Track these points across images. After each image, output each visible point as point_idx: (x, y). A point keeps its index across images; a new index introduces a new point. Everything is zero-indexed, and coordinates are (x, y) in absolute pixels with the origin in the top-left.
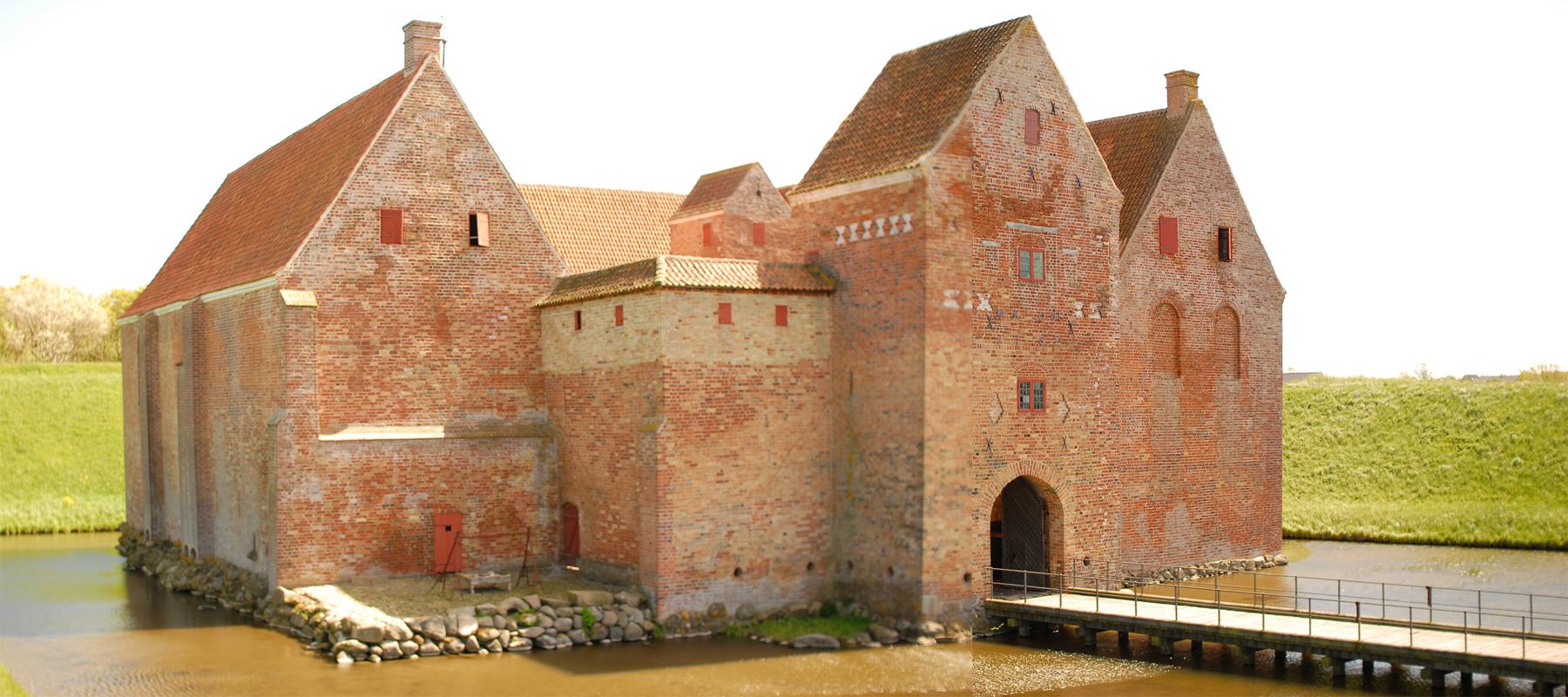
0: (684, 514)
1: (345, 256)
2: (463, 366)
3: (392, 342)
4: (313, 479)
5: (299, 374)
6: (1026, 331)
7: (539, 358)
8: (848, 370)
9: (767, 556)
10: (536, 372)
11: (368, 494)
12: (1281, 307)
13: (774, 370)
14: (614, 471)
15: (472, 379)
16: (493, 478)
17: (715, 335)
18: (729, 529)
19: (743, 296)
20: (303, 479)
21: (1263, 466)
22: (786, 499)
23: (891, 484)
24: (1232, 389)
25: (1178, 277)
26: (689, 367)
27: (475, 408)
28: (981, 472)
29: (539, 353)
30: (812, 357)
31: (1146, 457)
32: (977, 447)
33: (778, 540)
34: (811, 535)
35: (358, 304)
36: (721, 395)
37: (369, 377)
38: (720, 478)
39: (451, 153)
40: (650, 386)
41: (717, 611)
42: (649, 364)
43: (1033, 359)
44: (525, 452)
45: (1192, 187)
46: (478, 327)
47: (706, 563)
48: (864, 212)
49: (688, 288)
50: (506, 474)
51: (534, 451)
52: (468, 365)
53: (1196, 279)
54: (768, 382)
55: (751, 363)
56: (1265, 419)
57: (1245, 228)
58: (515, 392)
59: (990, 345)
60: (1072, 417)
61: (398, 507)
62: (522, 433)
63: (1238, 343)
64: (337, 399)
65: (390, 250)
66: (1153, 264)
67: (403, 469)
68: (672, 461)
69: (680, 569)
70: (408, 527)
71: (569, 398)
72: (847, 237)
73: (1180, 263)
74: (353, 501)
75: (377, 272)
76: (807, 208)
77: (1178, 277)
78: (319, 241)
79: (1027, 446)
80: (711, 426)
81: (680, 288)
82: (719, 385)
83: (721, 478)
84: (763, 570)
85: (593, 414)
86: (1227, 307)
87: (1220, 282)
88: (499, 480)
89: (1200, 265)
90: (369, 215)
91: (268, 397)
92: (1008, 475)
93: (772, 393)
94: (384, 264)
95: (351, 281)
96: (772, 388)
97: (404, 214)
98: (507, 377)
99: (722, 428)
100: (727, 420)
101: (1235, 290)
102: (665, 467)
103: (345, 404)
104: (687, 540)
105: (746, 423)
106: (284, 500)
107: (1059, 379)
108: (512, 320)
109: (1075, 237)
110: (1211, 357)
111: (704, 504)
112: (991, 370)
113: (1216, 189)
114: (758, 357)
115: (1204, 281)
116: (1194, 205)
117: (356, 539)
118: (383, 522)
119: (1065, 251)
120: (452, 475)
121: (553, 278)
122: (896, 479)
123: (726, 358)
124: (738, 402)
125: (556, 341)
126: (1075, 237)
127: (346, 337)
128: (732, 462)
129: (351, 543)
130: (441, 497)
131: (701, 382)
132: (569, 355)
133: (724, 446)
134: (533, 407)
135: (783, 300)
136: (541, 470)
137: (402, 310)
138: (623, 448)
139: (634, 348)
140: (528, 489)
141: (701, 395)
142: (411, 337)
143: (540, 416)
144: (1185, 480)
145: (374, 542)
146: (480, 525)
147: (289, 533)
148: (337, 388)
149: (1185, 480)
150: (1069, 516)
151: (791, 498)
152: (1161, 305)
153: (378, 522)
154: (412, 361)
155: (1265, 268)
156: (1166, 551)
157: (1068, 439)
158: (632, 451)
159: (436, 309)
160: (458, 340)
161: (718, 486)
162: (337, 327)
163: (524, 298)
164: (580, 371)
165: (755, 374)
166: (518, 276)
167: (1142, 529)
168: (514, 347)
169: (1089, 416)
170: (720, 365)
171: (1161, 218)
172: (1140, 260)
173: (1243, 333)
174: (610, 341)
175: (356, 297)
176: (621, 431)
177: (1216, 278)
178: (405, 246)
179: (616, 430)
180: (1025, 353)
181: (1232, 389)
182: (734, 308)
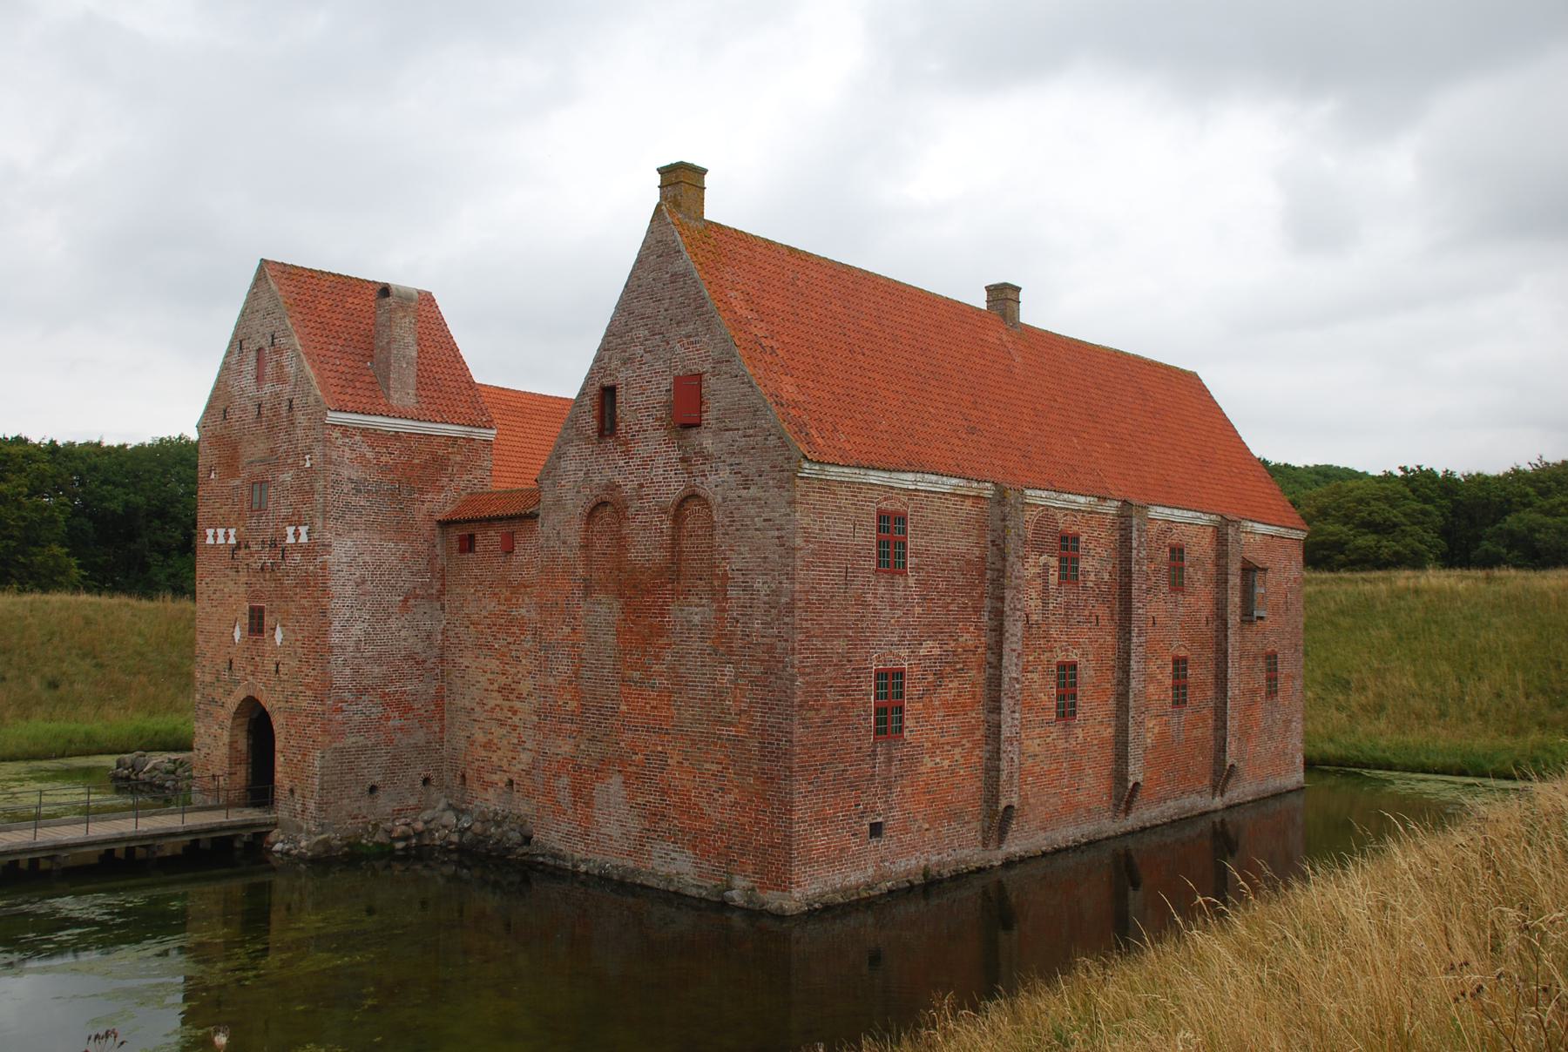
21: (754, 744)
24: (696, 619)
25: (621, 463)
28: (227, 688)
31: (572, 705)
45: (643, 333)
53: (646, 462)
56: (757, 670)
60: (284, 643)
66: (588, 452)
73: (626, 444)
77: (621, 463)
79: (252, 668)
87: (683, 460)
109: (289, 461)
113: (678, 323)
115: (660, 461)
126: (289, 461)
149: (622, 744)
157: (280, 665)
167: (565, 797)
169: (297, 643)
172: (572, 451)
177: (675, 455)
181: (696, 619)
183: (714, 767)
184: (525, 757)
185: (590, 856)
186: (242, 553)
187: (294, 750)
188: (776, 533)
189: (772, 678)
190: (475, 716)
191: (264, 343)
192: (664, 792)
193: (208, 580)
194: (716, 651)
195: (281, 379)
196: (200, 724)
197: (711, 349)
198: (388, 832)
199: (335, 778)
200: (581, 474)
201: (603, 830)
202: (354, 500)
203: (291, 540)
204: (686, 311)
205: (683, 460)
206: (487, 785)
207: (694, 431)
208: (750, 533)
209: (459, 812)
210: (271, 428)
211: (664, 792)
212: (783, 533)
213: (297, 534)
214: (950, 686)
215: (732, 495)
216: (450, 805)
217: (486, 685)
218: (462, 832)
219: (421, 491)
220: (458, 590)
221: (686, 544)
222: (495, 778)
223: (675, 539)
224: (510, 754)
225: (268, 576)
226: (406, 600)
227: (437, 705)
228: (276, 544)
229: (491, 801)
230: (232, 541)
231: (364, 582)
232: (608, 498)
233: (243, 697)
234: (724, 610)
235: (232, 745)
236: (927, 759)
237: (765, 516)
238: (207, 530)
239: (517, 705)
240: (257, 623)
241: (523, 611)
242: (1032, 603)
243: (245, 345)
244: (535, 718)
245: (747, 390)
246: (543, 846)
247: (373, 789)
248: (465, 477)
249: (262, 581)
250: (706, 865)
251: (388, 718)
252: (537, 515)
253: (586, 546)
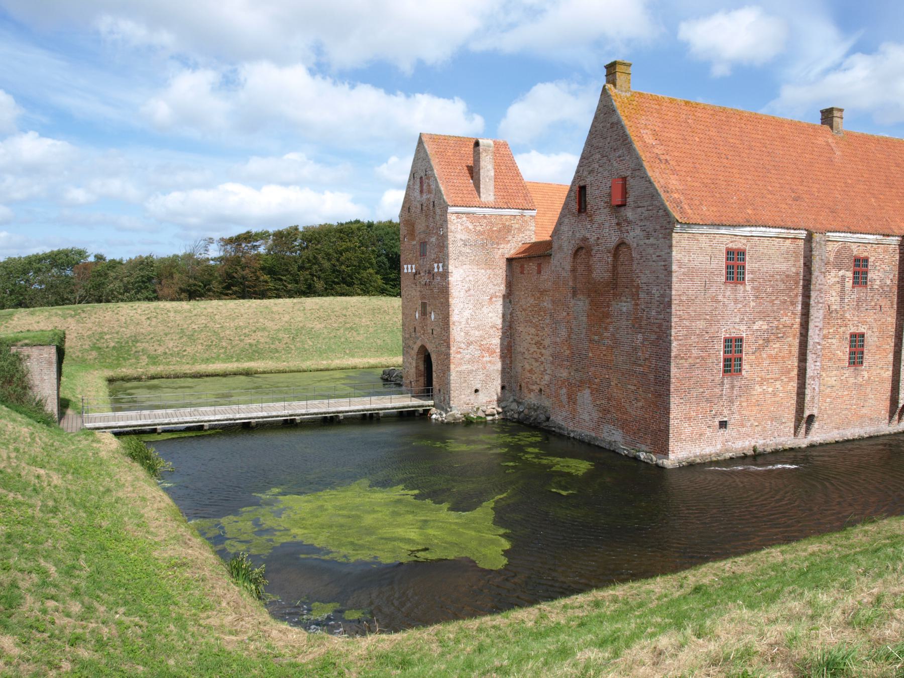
21: (651, 377)
24: (624, 309)
25: (589, 227)
56: (653, 337)
57: (637, 173)
73: (591, 216)
87: (618, 224)
89: (603, 216)
101: (629, 228)
113: (615, 150)
115: (607, 225)
116: (601, 169)
144: (590, 373)
149: (590, 373)
155: (655, 203)
167: (564, 398)
177: (614, 221)
181: (624, 309)
183: (633, 388)
184: (547, 378)
185: (576, 429)
186: (418, 276)
188: (663, 263)
189: (661, 342)
190: (525, 356)
191: (423, 174)
192: (609, 399)
194: (633, 326)
195: (429, 192)
197: (630, 163)
198: (484, 412)
199: (457, 385)
200: (571, 233)
201: (581, 417)
202: (463, 249)
203: (436, 270)
204: (619, 143)
205: (618, 224)
206: (531, 391)
207: (623, 208)
208: (651, 263)
209: (519, 403)
212: (666, 263)
214: (774, 346)
215: (641, 243)
216: (515, 400)
217: (530, 341)
218: (520, 413)
219: (498, 244)
220: (517, 293)
221: (620, 269)
222: (534, 387)
223: (615, 267)
224: (540, 376)
226: (491, 298)
227: (508, 350)
228: (429, 271)
229: (532, 399)
230: (414, 271)
231: (469, 290)
232: (583, 245)
233: (420, 345)
235: (417, 367)
236: (757, 387)
237: (658, 254)
239: (543, 351)
241: (545, 304)
242: (833, 299)
244: (551, 358)
245: (648, 185)
246: (555, 423)
247: (476, 391)
248: (521, 235)
250: (628, 438)
251: (483, 357)
252: (551, 255)
253: (574, 270)
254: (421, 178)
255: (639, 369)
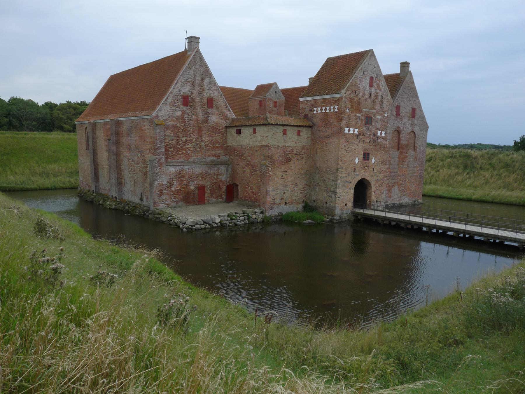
0: (273, 188)
1: (172, 109)
2: (206, 144)
3: (186, 136)
4: (164, 177)
5: (160, 145)
6: (366, 139)
7: (226, 142)
8: (316, 148)
9: (293, 199)
10: (225, 146)
11: (179, 181)
12: (427, 131)
13: (296, 148)
14: (251, 175)
15: (208, 148)
16: (214, 176)
17: (282, 138)
18: (284, 192)
19: (289, 127)
20: (161, 177)
21: (419, 176)
22: (298, 183)
23: (327, 180)
24: (412, 154)
25: (400, 122)
26: (276, 147)
27: (209, 156)
28: (353, 177)
29: (226, 140)
30: (306, 144)
31: (388, 173)
32: (352, 170)
33: (296, 194)
34: (304, 193)
35: (176, 124)
36: (283, 155)
37: (179, 147)
38: (282, 178)
39: (203, 79)
40: (264, 152)
41: (280, 214)
42: (264, 146)
43: (367, 147)
44: (223, 169)
46: (210, 132)
47: (278, 201)
48: (323, 105)
49: (276, 125)
50: (217, 175)
51: (226, 169)
52: (207, 144)
53: (405, 123)
54: (295, 151)
55: (291, 146)
56: (420, 163)
58: (220, 151)
59: (357, 143)
60: (376, 163)
61: (188, 185)
62: (222, 163)
63: (415, 141)
64: (170, 153)
65: (185, 108)
67: (189, 174)
68: (271, 173)
69: (272, 203)
70: (191, 191)
71: (236, 153)
72: (317, 111)
74: (175, 183)
75: (181, 115)
76: (305, 102)
77: (400, 122)
78: (165, 105)
79: (364, 170)
80: (280, 164)
81: (274, 125)
82: (283, 152)
83: (282, 178)
84: (291, 203)
85: (244, 159)
86: (413, 132)
88: (216, 177)
89: (406, 120)
90: (179, 97)
91: (148, 152)
92: (359, 178)
93: (296, 154)
94: (183, 112)
95: (174, 117)
96: (296, 153)
97: (190, 97)
98: (217, 147)
99: (283, 164)
100: (284, 162)
101: (415, 126)
102: (269, 175)
103: (172, 155)
104: (273, 195)
105: (289, 162)
106: (155, 183)
107: (373, 152)
108: (219, 130)
109: (380, 113)
110: (407, 145)
111: (278, 185)
112: (357, 150)
114: (293, 144)
115: (407, 124)
117: (176, 194)
118: (184, 189)
119: (377, 117)
120: (203, 176)
121: (230, 118)
122: (329, 179)
123: (285, 145)
124: (287, 157)
125: (232, 137)
126: (380, 113)
127: (173, 134)
128: (285, 173)
129: (175, 195)
130: (200, 182)
131: (278, 151)
132: (237, 141)
133: (283, 168)
134: (225, 156)
135: (299, 129)
136: (227, 174)
137: (189, 127)
138: (254, 169)
139: (259, 141)
140: (223, 179)
141: (278, 155)
142: (191, 135)
143: (226, 158)
145: (181, 195)
146: (210, 190)
147: (157, 193)
148: (170, 149)
150: (373, 190)
151: (299, 183)
152: (395, 131)
153: (182, 189)
154: (191, 142)
156: (392, 199)
158: (257, 170)
159: (198, 126)
160: (204, 136)
161: (282, 180)
162: (170, 131)
163: (222, 124)
164: (240, 146)
165: (292, 149)
166: (221, 117)
168: (219, 138)
170: (283, 146)
171: (397, 105)
173: (416, 139)
174: (251, 138)
175: (175, 122)
176: (254, 164)
177: (410, 123)
178: (189, 107)
179: (252, 163)
180: (365, 145)
181: (412, 154)
182: (287, 130)
183: (413, 181)
186: (361, 137)
187: (378, 190)
193: (345, 144)
195: (379, 88)
196: (340, 190)
203: (379, 135)
210: (374, 102)
211: (405, 187)
213: (381, 133)
215: (419, 132)
225: (371, 144)
228: (375, 135)
230: (356, 132)
234: (416, 153)
238: (346, 129)
240: (366, 157)
243: (365, 73)
249: (369, 145)
254: (372, 78)
255: (415, 174)
